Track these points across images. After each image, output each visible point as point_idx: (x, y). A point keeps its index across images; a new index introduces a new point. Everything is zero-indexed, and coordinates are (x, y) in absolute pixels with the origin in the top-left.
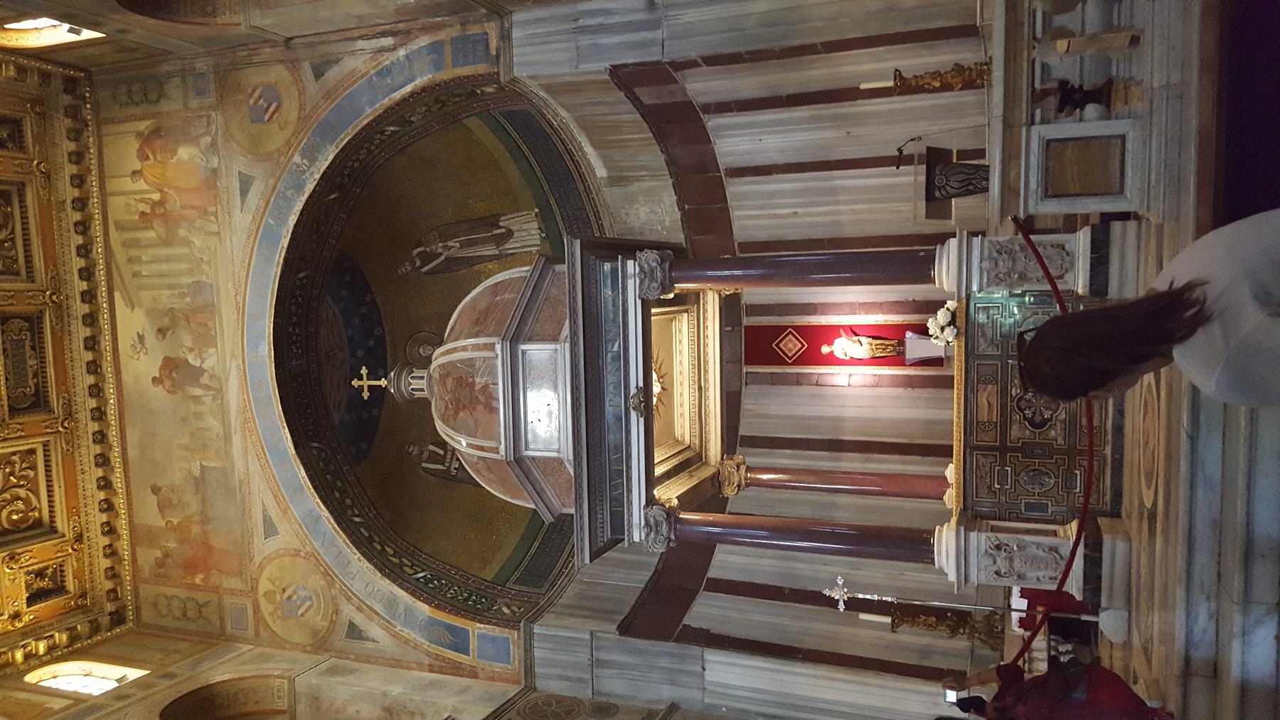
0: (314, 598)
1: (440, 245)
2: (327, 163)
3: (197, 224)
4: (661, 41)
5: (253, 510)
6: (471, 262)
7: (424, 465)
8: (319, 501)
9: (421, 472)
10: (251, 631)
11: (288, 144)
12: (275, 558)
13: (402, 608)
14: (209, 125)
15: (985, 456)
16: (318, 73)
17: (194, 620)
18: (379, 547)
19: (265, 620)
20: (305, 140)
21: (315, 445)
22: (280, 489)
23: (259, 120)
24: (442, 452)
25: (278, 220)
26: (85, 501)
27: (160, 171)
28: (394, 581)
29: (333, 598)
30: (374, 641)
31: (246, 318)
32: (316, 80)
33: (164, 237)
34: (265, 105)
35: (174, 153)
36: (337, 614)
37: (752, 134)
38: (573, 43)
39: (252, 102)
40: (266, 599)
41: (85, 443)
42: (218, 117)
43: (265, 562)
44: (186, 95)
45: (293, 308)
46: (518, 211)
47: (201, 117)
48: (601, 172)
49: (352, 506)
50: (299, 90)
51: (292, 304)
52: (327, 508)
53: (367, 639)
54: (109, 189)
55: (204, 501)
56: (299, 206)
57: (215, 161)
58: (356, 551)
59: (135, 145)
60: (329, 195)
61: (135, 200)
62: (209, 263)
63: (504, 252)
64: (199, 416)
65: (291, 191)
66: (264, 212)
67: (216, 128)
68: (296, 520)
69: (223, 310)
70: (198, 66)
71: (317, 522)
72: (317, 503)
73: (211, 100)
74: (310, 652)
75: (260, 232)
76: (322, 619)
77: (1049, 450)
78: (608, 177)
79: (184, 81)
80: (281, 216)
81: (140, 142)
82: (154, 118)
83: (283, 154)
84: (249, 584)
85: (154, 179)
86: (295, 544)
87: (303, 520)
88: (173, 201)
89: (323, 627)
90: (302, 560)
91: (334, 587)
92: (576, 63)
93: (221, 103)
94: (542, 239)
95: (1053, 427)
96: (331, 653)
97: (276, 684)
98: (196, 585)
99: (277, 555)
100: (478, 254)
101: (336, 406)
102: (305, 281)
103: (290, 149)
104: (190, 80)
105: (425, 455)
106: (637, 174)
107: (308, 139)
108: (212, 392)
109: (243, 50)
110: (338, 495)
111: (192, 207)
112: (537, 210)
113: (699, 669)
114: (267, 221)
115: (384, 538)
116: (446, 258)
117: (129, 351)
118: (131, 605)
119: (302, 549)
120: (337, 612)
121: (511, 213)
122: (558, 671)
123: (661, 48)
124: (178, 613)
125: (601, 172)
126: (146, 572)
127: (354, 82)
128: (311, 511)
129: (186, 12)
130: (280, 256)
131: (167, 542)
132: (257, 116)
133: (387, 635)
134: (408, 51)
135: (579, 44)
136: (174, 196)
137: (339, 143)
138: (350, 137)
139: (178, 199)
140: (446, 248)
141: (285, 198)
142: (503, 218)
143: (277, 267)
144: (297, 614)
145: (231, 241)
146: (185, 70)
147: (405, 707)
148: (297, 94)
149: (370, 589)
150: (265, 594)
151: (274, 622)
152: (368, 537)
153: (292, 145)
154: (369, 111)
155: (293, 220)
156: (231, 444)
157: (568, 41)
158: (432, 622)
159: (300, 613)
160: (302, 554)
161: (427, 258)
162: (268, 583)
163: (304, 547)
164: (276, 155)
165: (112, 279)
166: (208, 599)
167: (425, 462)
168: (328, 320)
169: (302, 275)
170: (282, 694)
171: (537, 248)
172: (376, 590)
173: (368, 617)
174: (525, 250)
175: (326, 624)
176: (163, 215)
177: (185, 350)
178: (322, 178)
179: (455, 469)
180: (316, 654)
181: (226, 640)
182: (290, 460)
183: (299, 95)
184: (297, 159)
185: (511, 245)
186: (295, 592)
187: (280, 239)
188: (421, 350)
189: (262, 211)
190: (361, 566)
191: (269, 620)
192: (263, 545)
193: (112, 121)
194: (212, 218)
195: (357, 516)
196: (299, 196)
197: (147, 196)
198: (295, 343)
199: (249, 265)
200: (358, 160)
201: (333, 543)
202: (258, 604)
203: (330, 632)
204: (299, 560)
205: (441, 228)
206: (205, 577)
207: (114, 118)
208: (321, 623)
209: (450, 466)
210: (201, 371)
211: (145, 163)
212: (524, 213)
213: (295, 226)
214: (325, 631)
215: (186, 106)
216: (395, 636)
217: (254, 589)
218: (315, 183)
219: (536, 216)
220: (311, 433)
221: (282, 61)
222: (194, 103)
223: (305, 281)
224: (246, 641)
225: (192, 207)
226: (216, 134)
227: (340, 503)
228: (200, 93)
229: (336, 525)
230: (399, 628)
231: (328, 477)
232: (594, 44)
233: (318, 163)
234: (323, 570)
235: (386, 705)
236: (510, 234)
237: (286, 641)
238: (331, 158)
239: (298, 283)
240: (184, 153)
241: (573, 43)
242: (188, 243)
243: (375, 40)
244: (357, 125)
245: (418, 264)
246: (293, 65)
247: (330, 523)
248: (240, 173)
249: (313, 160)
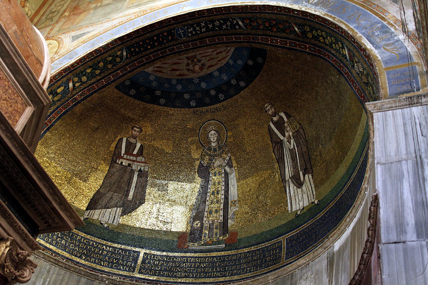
1: (291, 134)
2: (313, 12)
4: (403, 239)
6: (281, 160)
7: (125, 140)
9: (119, 138)
21: (125, 54)
24: (135, 152)
38: (404, 157)
45: (217, 23)
46: (315, 187)
48: (337, 246)
49: (81, 81)
51: (219, 21)
78: (334, 253)
92: (384, 162)
100: (286, 164)
101: (159, 69)
102: (237, 27)
105: (132, 140)
106: (334, 278)
110: (89, 71)
112: (316, 202)
115: (58, 104)
116: (282, 141)
121: (314, 182)
123: (395, 240)
125: (337, 246)
127: (377, 14)
134: (403, 41)
135: (404, 162)
140: (289, 138)
142: (310, 176)
143: (241, 3)
152: (56, 92)
157: (407, 154)
161: (280, 125)
167: (127, 140)
168: (218, 53)
169: (240, 23)
171: (289, 210)
174: (289, 200)
179: (122, 163)
185: (292, 188)
188: (213, 132)
195: (74, 86)
198: (195, 29)
205: (302, 131)
209: (124, 159)
212: (314, 193)
219: (313, 203)
220: (133, 49)
223: (237, 27)
227: (82, 72)
231: (101, 64)
232: (403, 176)
236: (299, 184)
238: (317, 13)
239: (235, 22)
241: (404, 157)
244: (341, 22)
245: (275, 119)
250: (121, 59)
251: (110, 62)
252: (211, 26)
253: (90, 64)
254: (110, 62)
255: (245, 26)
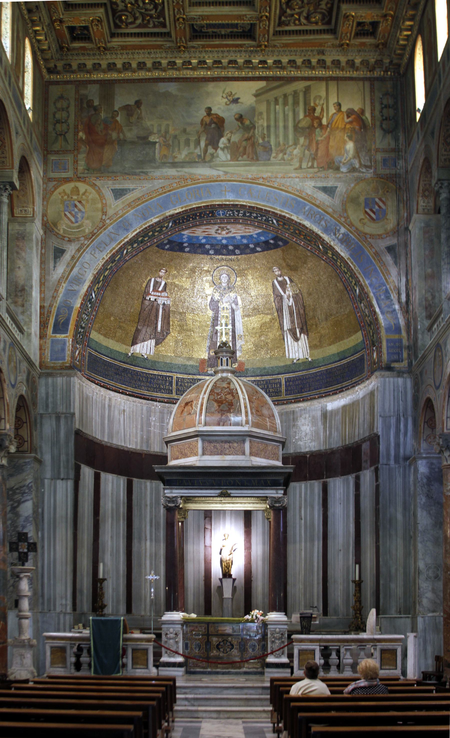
0: (77, 224)
2: (339, 251)
3: (306, 152)
5: (129, 181)
8: (138, 231)
10: (52, 175)
11: (351, 225)
12: (99, 195)
13: (76, 288)
14: (366, 167)
15: (205, 628)
16: (390, 249)
17: (54, 129)
18: (109, 267)
19: (60, 186)
20: (353, 237)
21: (170, 224)
22: (143, 202)
23: (366, 205)
25: (307, 213)
26: (130, 53)
27: (340, 126)
28: (92, 283)
29: (78, 239)
30: (55, 267)
31: (249, 184)
32: (386, 248)
33: (300, 125)
34: (374, 210)
35: (350, 138)
36: (69, 241)
37: (344, 500)
39: (377, 200)
40: (73, 188)
41: (168, 56)
42: (369, 174)
43: (97, 188)
44: (384, 151)
45: (255, 215)
47: (371, 163)
50: (381, 235)
51: (257, 214)
52: (134, 236)
53: (55, 263)
54: (331, 83)
55: (133, 143)
56: (316, 229)
57: (344, 169)
58: (108, 256)
59: (357, 108)
60: (322, 245)
61: (323, 104)
62: (283, 159)
63: (285, 333)
64: (187, 143)
65: (324, 224)
66: (313, 204)
67: (363, 173)
68: (125, 214)
69: (253, 168)
70: (401, 162)
71: (125, 229)
72: (136, 230)
73: (382, 171)
74: (43, 220)
75: (301, 200)
76: (64, 230)
77: (208, 650)
79: (393, 150)
80: (310, 216)
81: (358, 112)
82: (372, 124)
83: (346, 220)
84: (82, 175)
85: (335, 121)
86: (110, 212)
87: (125, 218)
88: (321, 134)
89: (59, 231)
90: (100, 217)
91: (85, 240)
93: (379, 176)
94: (293, 360)
95: (217, 652)
96: (44, 236)
97: (29, 209)
98: (78, 132)
99: (102, 197)
103: (349, 225)
104: (393, 155)
107: (354, 239)
108: (202, 155)
109: (407, 197)
110: (140, 239)
111: (317, 149)
113: (62, 476)
114: (308, 205)
117: (227, 90)
118: (60, 78)
119: (107, 217)
120: (70, 241)
122: (51, 392)
124: (58, 116)
126: (83, 92)
128: (131, 225)
129: (425, 181)
130: (286, 213)
131: (104, 110)
132: (369, 203)
133: (59, 277)
136: (324, 136)
137: (350, 261)
138: (353, 268)
139: (322, 138)
141: (321, 220)
144: (66, 211)
145: (296, 177)
146: (399, 152)
147: (26, 301)
148: (379, 233)
149: (86, 265)
150: (77, 188)
151: (60, 194)
153: (351, 228)
154: (367, 282)
155: (307, 223)
156: (169, 167)
158: (70, 309)
159: (67, 213)
160: (104, 217)
162: (84, 190)
163: (108, 219)
164: (345, 215)
165: (273, 80)
166: (69, 142)
169: (275, 221)
170: (23, 213)
172: (86, 270)
173: (69, 263)
175: (61, 232)
176: (313, 126)
177: (229, 135)
178: (330, 246)
180: (43, 225)
181: (44, 155)
182: (162, 211)
183: (379, 235)
184: (343, 230)
186: (80, 210)
187: (295, 213)
189: (314, 202)
190: (99, 260)
191: (60, 189)
192: (108, 188)
193: (372, 90)
194: (310, 164)
195: (127, 252)
196: (321, 230)
197: (325, 115)
198: (233, 213)
199: (281, 190)
200: (341, 265)
201: (112, 240)
202: (70, 181)
203: (57, 235)
204: (100, 213)
206: (83, 141)
207: (374, 92)
208: (62, 227)
210: (216, 147)
211: (345, 114)
213: (304, 226)
214: (57, 231)
215: (377, 150)
216: (59, 282)
217: (79, 179)
218: (328, 242)
221: (398, 224)
222: (379, 157)
224: (45, 172)
225: (317, 149)
226: (360, 172)
227: (135, 241)
228: (385, 161)
229: (123, 242)
230: (64, 285)
233: (340, 244)
234: (95, 231)
235: (26, 288)
237: (48, 202)
240: (350, 146)
242: (296, 143)
243: (405, 290)
246: (396, 232)
247: (125, 238)
248: (336, 187)
249: (342, 241)
250: (167, 228)
251: (157, 231)
252: (247, 214)
253: (143, 235)
254: (157, 231)
255: (278, 225)
